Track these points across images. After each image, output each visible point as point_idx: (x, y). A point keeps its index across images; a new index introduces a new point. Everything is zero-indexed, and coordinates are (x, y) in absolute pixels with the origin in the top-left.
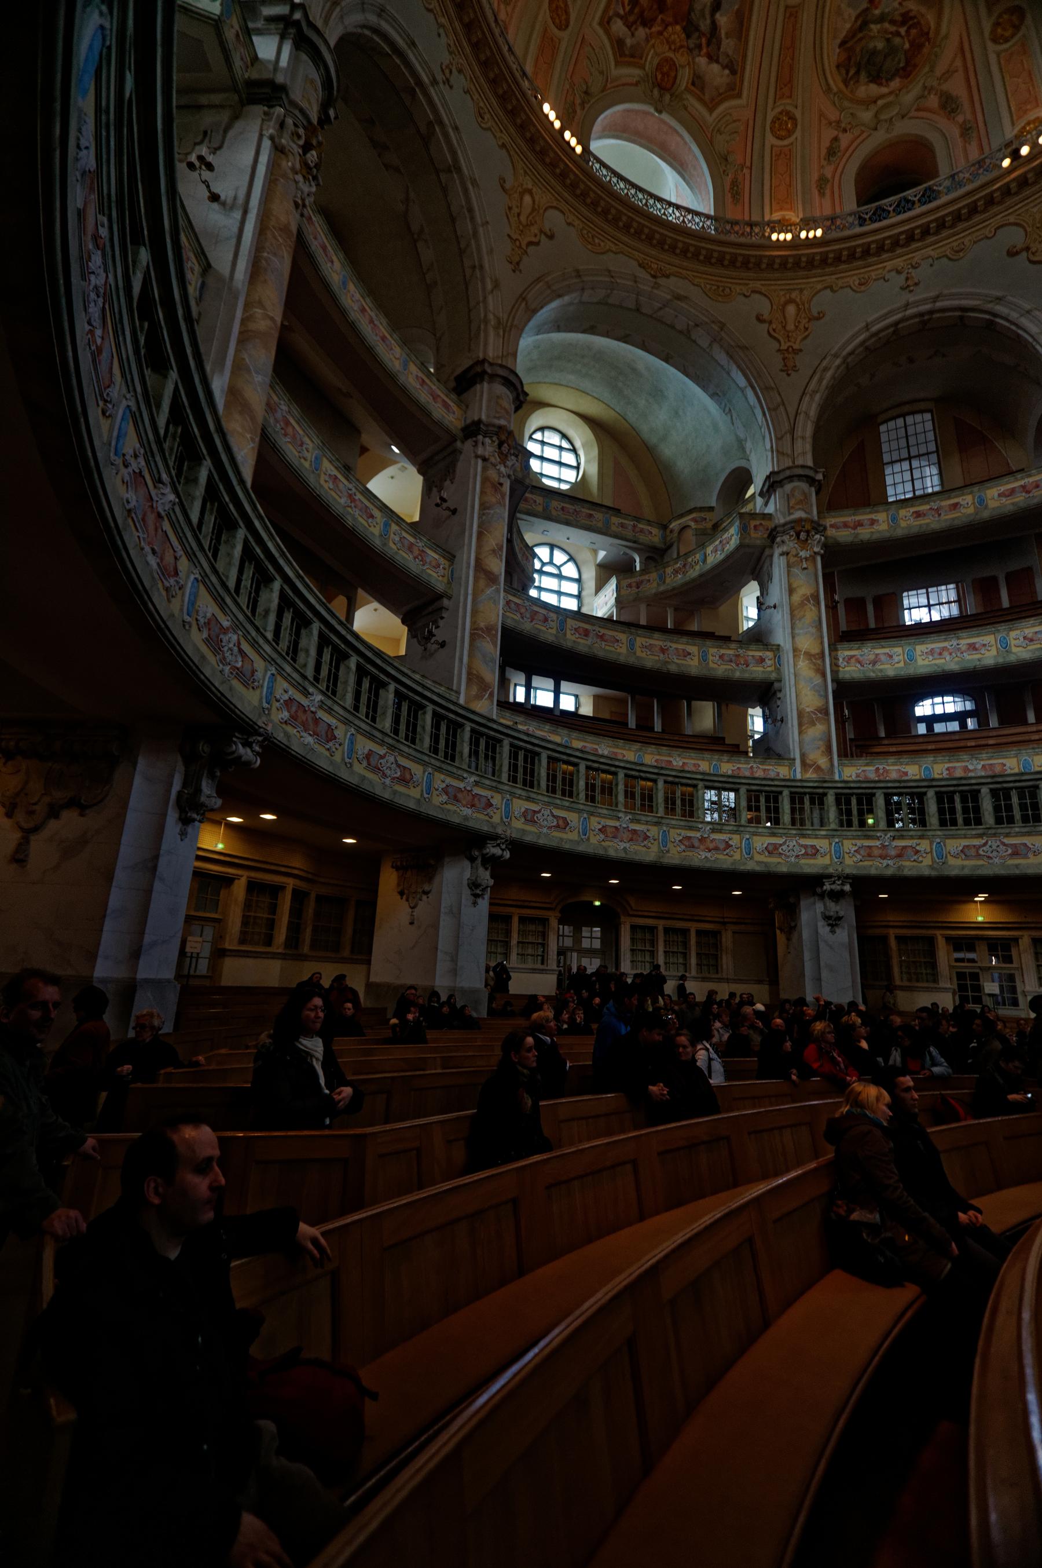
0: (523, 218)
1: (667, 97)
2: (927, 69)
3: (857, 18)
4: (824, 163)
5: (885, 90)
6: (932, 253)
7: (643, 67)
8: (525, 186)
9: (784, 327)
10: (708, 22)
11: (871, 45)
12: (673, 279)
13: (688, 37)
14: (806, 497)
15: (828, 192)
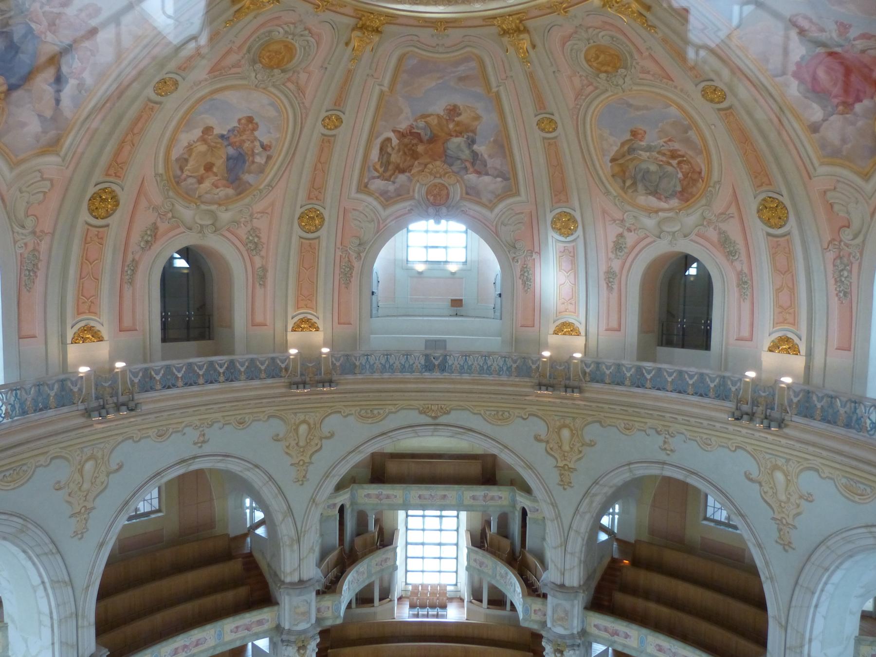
0: (301, 444)
1: (444, 210)
2: (704, 202)
3: (623, 144)
4: (611, 255)
5: (663, 205)
6: (686, 432)
7: (413, 198)
8: (298, 421)
9: (560, 447)
10: (467, 152)
11: (644, 166)
12: (453, 412)
13: (451, 165)
14: (567, 614)
15: (615, 287)
